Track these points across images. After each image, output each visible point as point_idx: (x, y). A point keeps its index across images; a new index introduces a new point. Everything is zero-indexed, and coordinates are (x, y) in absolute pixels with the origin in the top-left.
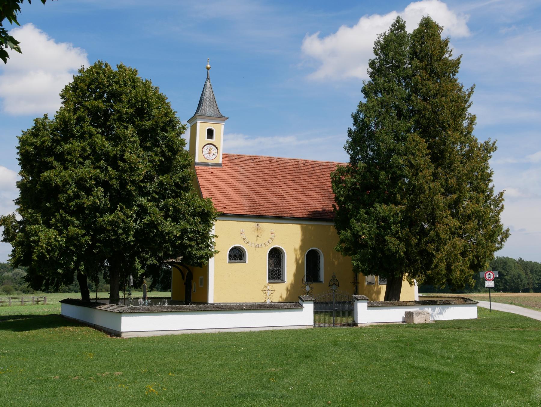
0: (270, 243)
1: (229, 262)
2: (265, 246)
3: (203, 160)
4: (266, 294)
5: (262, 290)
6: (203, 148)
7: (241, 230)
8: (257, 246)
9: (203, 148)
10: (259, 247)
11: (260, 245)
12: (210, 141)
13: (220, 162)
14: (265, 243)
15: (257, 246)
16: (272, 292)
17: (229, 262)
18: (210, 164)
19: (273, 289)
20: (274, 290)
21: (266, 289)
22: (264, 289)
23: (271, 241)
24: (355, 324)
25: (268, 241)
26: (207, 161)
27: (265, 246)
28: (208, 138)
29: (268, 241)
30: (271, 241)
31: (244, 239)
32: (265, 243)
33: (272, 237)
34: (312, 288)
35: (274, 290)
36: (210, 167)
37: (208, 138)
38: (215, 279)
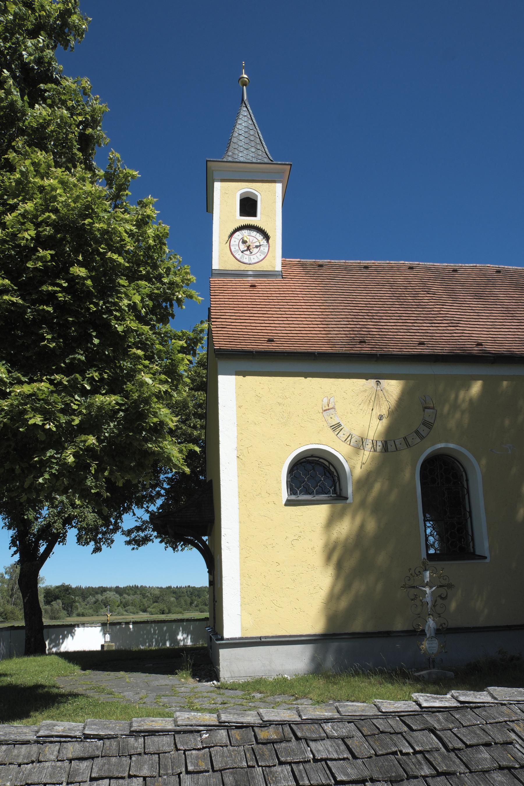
0: (422, 438)
1: (289, 503)
3: (232, 265)
7: (325, 400)
13: (278, 268)
17: (289, 503)
18: (250, 273)
23: (424, 430)
25: (417, 432)
26: (243, 267)
28: (242, 215)
30: (424, 430)
31: (336, 427)
33: (427, 419)
37: (242, 215)
38: (244, 559)
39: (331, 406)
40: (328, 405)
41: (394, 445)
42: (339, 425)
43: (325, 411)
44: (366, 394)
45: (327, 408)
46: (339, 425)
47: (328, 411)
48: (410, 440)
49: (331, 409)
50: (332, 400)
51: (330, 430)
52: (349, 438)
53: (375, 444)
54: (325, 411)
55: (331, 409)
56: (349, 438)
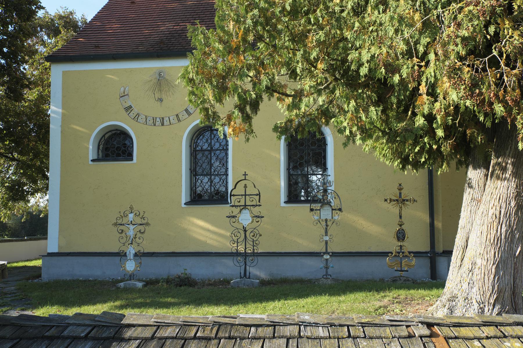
0: (189, 114)
2: (179, 120)
4: (123, 235)
5: (116, 224)
7: (122, 89)
8: (158, 123)
10: (163, 124)
11: (166, 119)
14: (177, 115)
15: (158, 123)
16: (142, 228)
19: (144, 222)
22: (120, 222)
25: (186, 110)
27: (179, 120)
29: (186, 110)
31: (129, 109)
32: (177, 115)
34: (256, 216)
35: (147, 224)
39: (126, 93)
40: (124, 93)
41: (168, 120)
42: (130, 107)
43: (121, 97)
44: (152, 83)
45: (123, 95)
46: (130, 107)
47: (123, 97)
48: (180, 116)
49: (126, 95)
50: (127, 89)
51: (124, 111)
52: (137, 116)
53: (155, 120)
54: (121, 97)
55: (126, 95)
56: (137, 116)
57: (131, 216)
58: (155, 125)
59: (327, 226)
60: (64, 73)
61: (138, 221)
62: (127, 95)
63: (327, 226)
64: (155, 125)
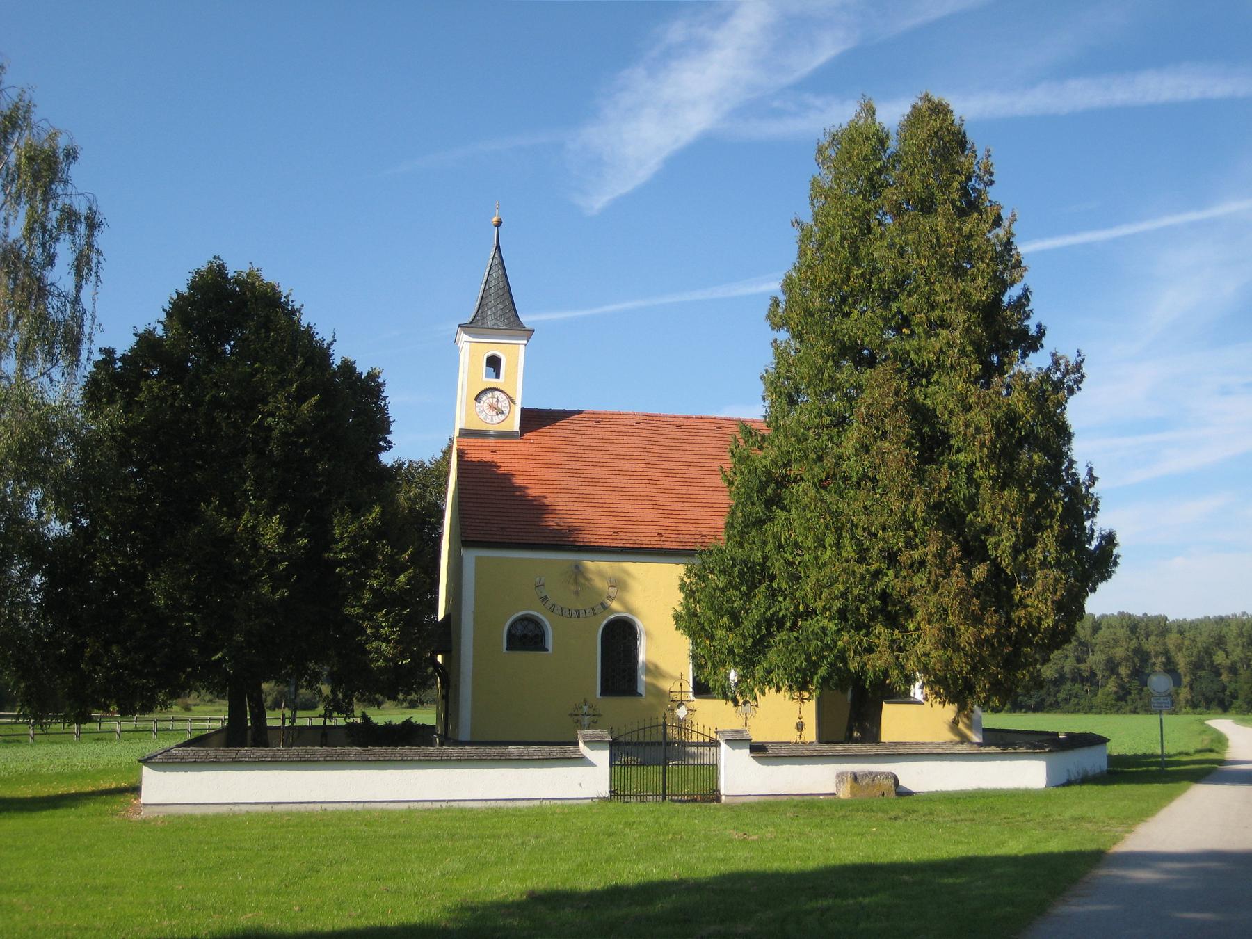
2: (595, 613)
4: (578, 724)
5: (571, 715)
6: (478, 398)
7: (538, 579)
9: (478, 398)
10: (579, 617)
11: (582, 612)
12: (493, 382)
14: (593, 609)
16: (595, 718)
18: (492, 433)
19: (595, 713)
20: (600, 715)
21: (580, 712)
22: (576, 713)
24: (714, 796)
26: (484, 427)
27: (595, 613)
32: (593, 609)
36: (492, 440)
48: (596, 610)
50: (543, 579)
57: (585, 708)
58: (570, 617)
59: (746, 718)
60: (477, 558)
61: (591, 712)
62: (543, 585)
63: (746, 718)
64: (570, 617)
